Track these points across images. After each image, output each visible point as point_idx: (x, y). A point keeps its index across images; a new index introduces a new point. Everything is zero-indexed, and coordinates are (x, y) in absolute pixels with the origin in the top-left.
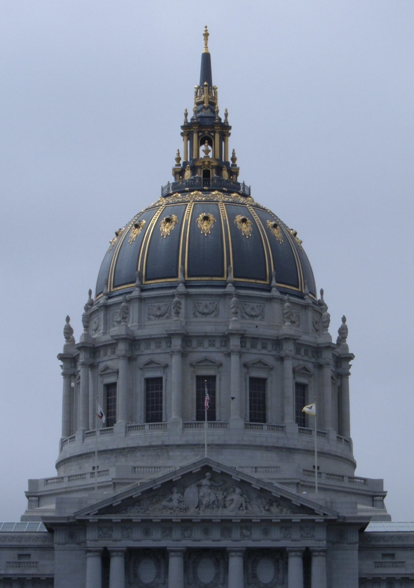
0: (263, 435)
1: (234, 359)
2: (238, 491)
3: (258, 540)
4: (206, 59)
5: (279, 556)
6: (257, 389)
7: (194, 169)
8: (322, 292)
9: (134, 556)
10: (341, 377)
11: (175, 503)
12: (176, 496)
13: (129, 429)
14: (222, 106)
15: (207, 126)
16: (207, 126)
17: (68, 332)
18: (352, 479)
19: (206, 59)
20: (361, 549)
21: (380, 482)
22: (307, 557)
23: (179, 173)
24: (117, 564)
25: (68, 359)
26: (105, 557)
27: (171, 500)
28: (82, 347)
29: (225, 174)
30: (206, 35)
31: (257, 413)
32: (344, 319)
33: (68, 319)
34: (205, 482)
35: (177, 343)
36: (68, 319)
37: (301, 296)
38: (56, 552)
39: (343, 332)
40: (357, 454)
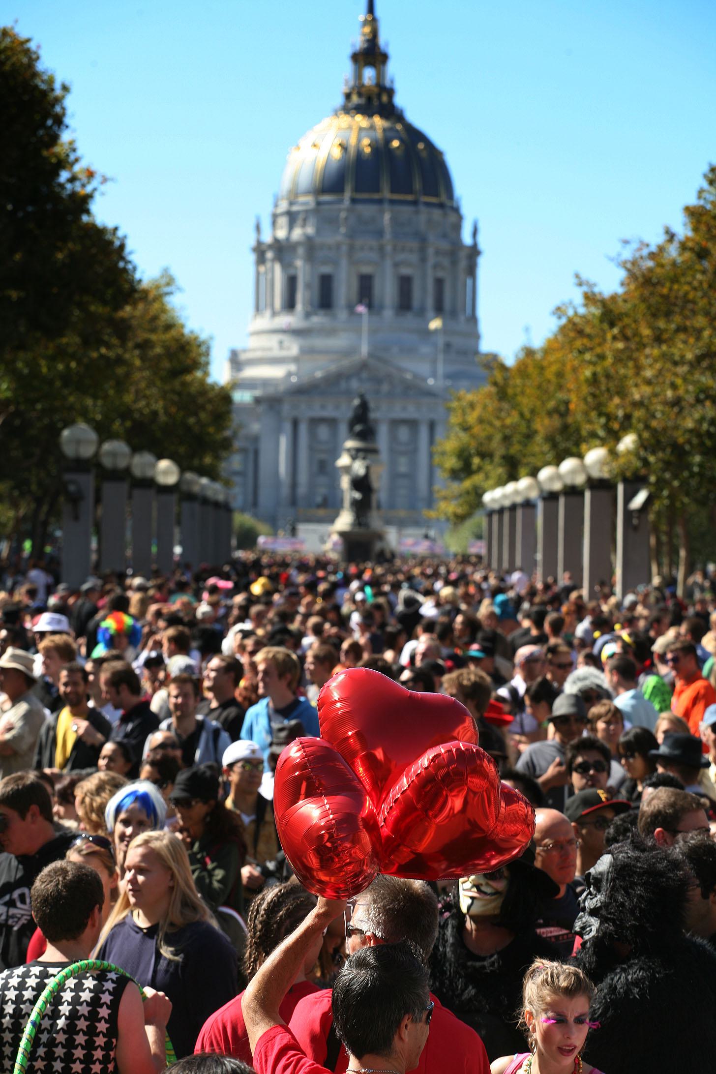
0: (409, 320)
1: (388, 263)
3: (398, 413)
5: (412, 424)
6: (405, 285)
7: (360, 95)
9: (315, 422)
10: (472, 270)
13: (307, 315)
14: (382, 40)
15: (371, 54)
16: (371, 54)
17: (258, 228)
18: (476, 352)
22: (432, 426)
23: (348, 96)
24: (303, 429)
25: (260, 251)
26: (295, 424)
28: (270, 247)
29: (385, 98)
31: (405, 304)
35: (344, 248)
37: (441, 206)
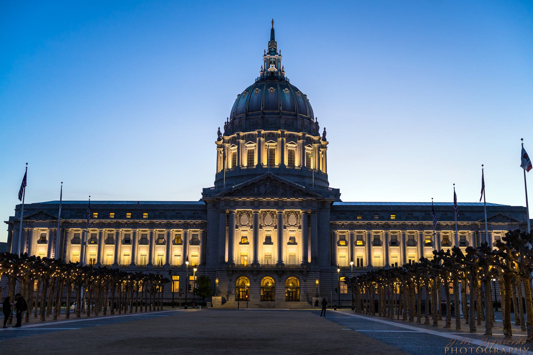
2: (281, 187)
4: (273, 31)
8: (316, 118)
11: (256, 192)
12: (256, 189)
17: (219, 133)
19: (273, 31)
20: (331, 212)
21: (338, 190)
27: (254, 191)
30: (273, 22)
32: (325, 129)
33: (219, 128)
34: (268, 183)
36: (219, 128)
38: (208, 212)
39: (325, 133)
40: (329, 180)
